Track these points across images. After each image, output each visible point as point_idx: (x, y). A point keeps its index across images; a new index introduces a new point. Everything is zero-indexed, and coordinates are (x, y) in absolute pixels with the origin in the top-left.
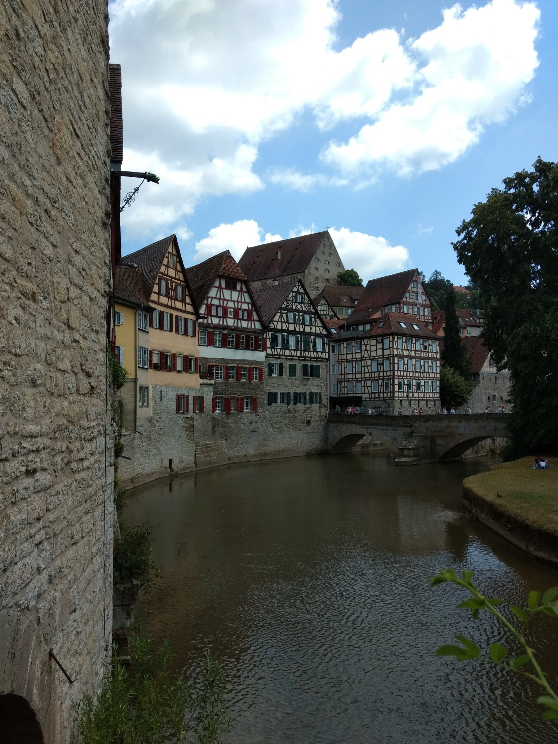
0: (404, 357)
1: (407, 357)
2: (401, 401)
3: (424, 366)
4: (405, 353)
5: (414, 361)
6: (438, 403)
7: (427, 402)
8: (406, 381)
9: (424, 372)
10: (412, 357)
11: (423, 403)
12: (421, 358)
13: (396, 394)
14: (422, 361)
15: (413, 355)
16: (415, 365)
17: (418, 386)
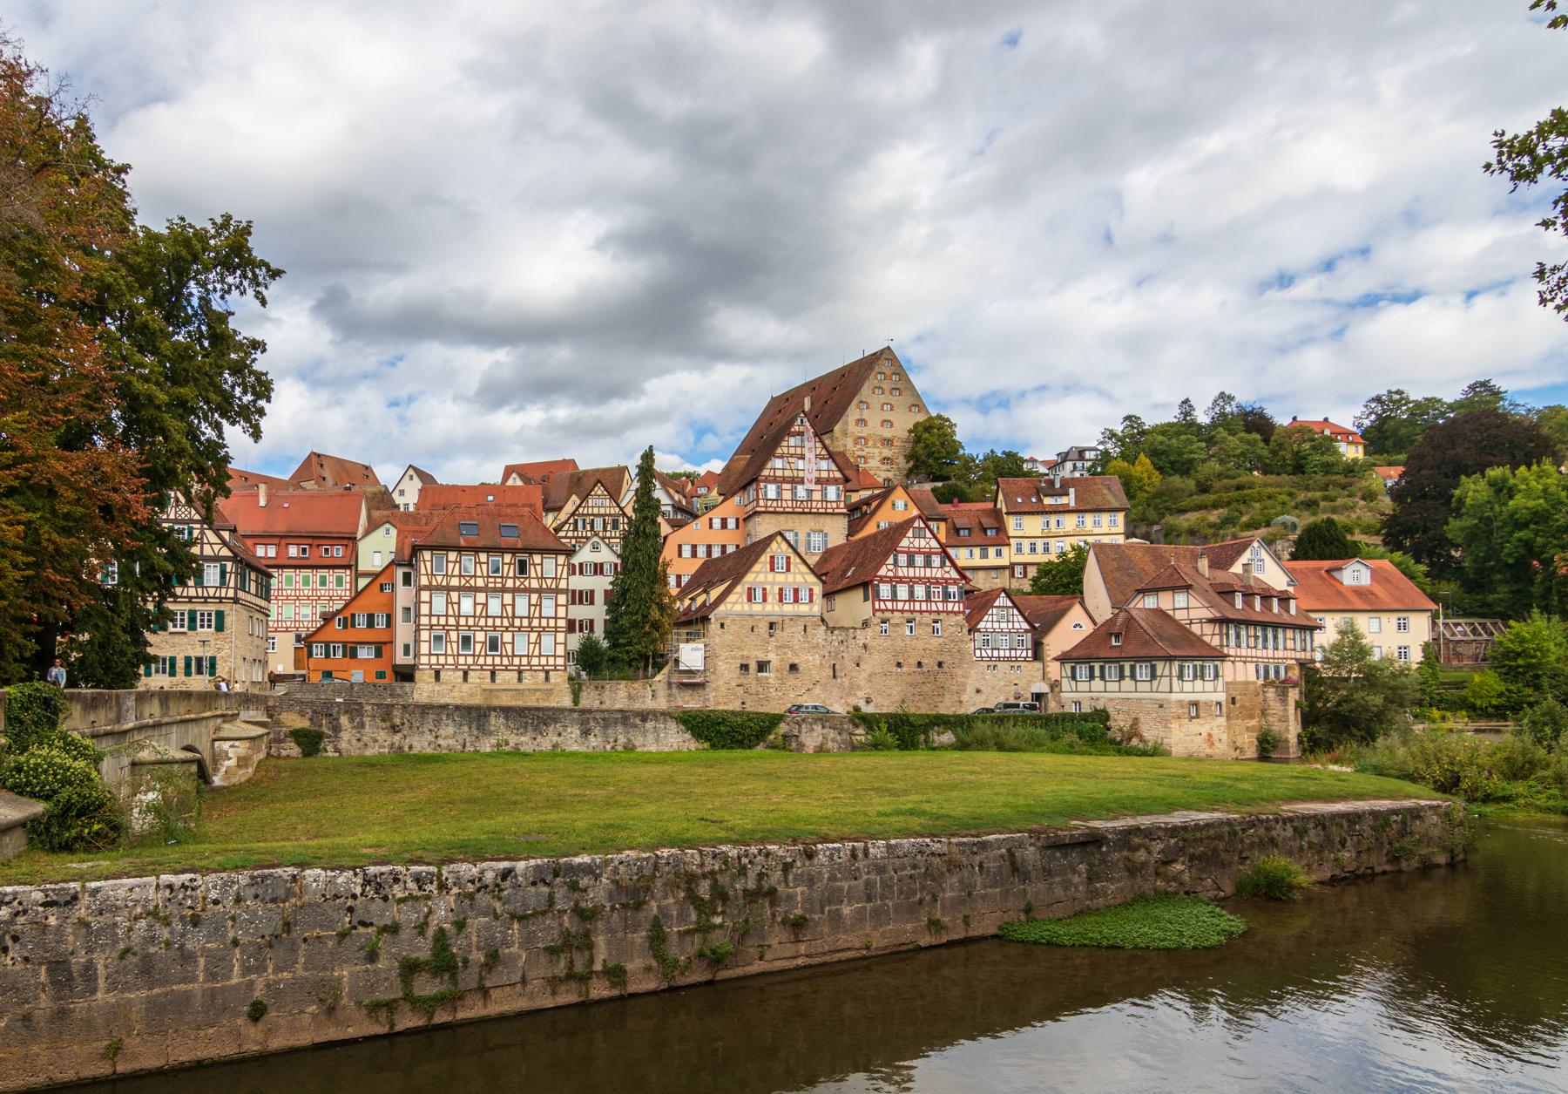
0: (448, 589)
1: (458, 589)
2: (437, 673)
3: (513, 605)
4: (455, 582)
5: (481, 597)
6: (558, 679)
7: (520, 672)
8: (454, 635)
9: (514, 617)
10: (477, 589)
11: (507, 678)
12: (504, 590)
13: (424, 660)
14: (508, 598)
15: (480, 583)
16: (485, 605)
17: (494, 645)
